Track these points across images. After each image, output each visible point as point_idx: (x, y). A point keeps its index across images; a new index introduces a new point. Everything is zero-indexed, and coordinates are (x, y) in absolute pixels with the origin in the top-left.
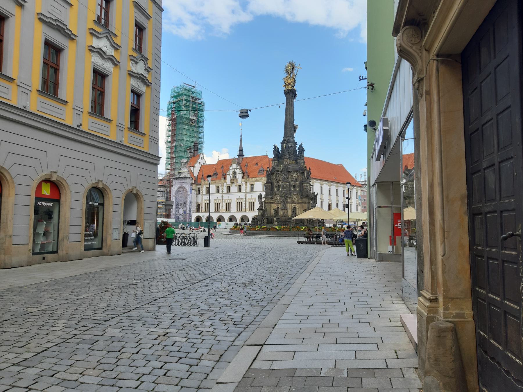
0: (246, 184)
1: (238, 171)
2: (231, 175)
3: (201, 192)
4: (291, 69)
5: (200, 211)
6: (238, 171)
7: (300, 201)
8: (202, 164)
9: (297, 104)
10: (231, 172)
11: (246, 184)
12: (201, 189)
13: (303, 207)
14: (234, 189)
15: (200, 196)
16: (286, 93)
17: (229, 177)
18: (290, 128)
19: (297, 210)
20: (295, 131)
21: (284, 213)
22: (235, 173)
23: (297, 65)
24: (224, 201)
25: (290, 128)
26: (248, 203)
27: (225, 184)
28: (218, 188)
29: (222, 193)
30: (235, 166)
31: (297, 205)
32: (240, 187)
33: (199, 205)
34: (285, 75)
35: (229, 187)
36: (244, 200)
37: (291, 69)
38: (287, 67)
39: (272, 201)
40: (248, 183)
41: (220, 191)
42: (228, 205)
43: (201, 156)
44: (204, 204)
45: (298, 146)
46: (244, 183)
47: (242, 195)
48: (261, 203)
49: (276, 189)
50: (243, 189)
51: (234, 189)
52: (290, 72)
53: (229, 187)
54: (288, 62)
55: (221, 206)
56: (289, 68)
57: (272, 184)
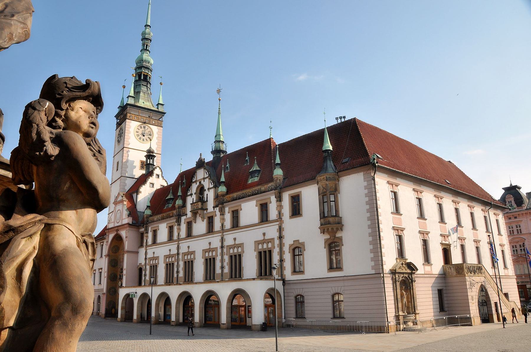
0: (222, 213)
1: (207, 184)
2: (194, 196)
3: (145, 241)
5: (143, 284)
6: (207, 184)
8: (157, 187)
10: (194, 188)
11: (222, 213)
12: (145, 235)
14: (200, 227)
15: (142, 251)
17: (190, 200)
22: (201, 190)
24: (180, 257)
26: (226, 258)
27: (183, 218)
28: (171, 229)
29: (179, 239)
30: (201, 174)
32: (211, 221)
33: (140, 270)
35: (189, 225)
36: (219, 251)
40: (227, 209)
41: (175, 237)
42: (189, 265)
43: (157, 171)
44: (148, 267)
46: (217, 210)
47: (215, 241)
50: (217, 226)
51: (200, 227)
53: (189, 225)
55: (175, 270)
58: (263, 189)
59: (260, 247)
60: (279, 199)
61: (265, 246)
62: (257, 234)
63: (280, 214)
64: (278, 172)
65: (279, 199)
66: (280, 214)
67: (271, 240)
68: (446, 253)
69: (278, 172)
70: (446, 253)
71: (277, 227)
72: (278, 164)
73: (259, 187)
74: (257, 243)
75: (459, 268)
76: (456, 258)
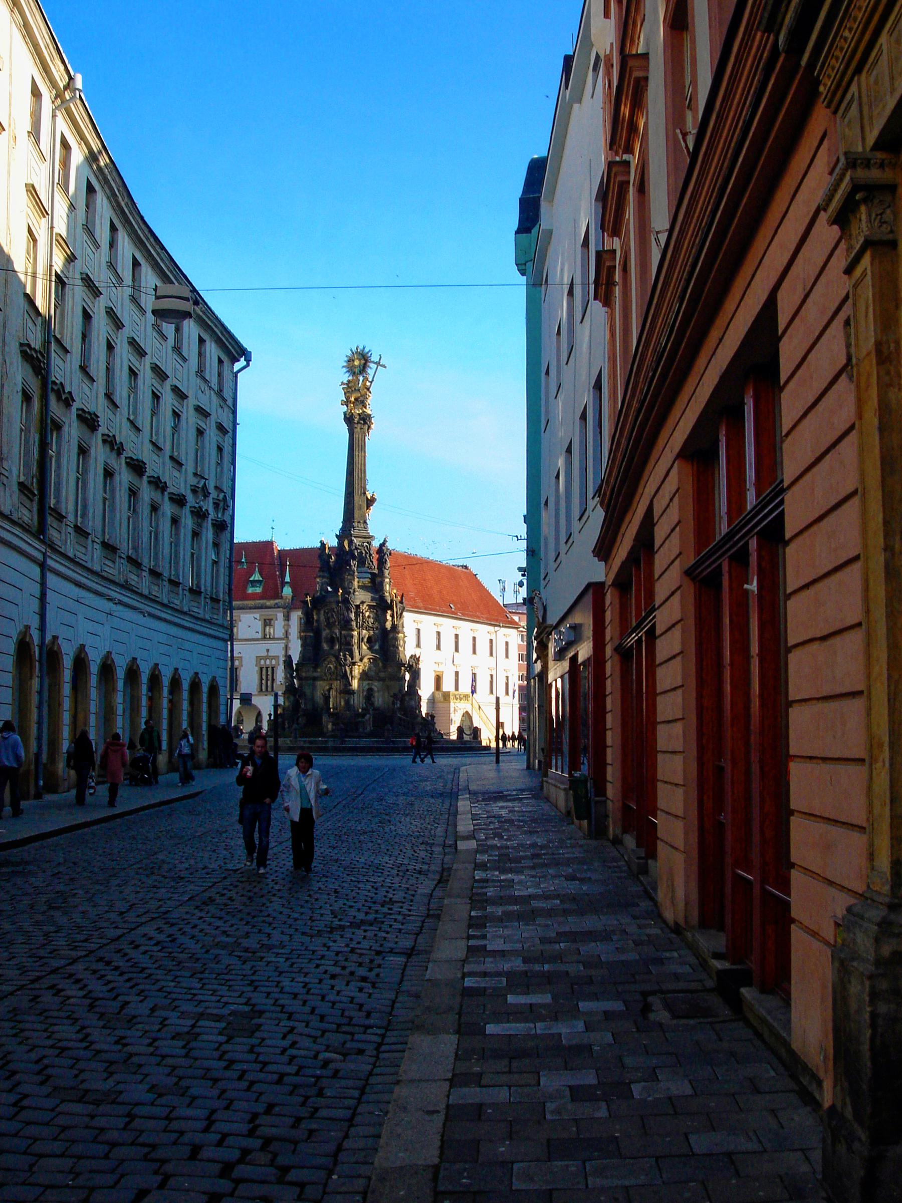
4: (360, 363)
7: (382, 675)
9: (373, 441)
13: (388, 688)
16: (349, 419)
18: (356, 501)
19: (376, 694)
20: (368, 507)
21: (347, 702)
23: (375, 358)
25: (356, 501)
31: (376, 683)
34: (346, 378)
37: (360, 363)
38: (350, 360)
39: (315, 674)
45: (376, 544)
48: (289, 678)
49: (325, 646)
52: (357, 370)
54: (354, 350)
56: (357, 363)
57: (318, 633)
58: (268, 603)
59: (262, 662)
60: (287, 618)
61: (268, 662)
62: (261, 649)
63: (287, 634)
64: (287, 591)
65: (287, 618)
66: (287, 634)
67: (276, 658)
68: (438, 680)
69: (287, 591)
70: (438, 680)
71: (283, 645)
72: (287, 583)
73: (264, 601)
74: (259, 658)
75: (446, 696)
76: (448, 685)
